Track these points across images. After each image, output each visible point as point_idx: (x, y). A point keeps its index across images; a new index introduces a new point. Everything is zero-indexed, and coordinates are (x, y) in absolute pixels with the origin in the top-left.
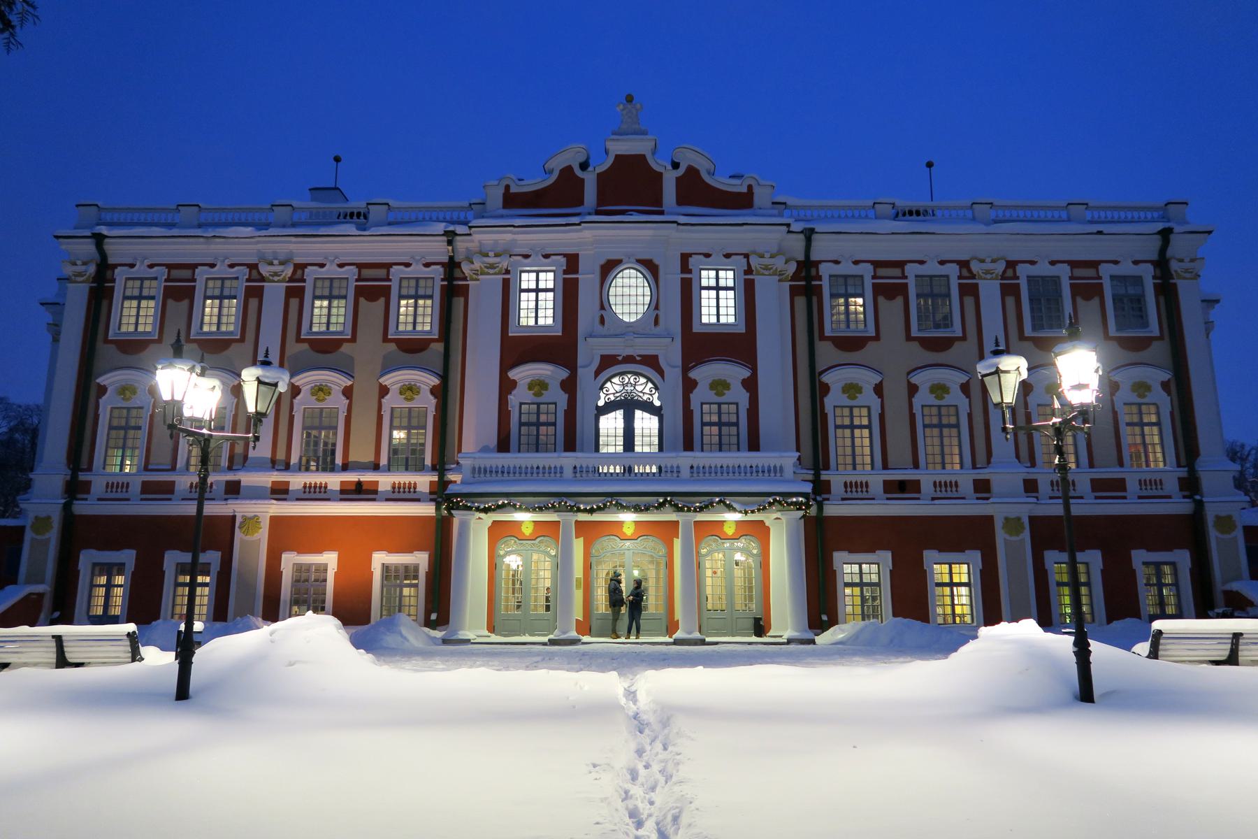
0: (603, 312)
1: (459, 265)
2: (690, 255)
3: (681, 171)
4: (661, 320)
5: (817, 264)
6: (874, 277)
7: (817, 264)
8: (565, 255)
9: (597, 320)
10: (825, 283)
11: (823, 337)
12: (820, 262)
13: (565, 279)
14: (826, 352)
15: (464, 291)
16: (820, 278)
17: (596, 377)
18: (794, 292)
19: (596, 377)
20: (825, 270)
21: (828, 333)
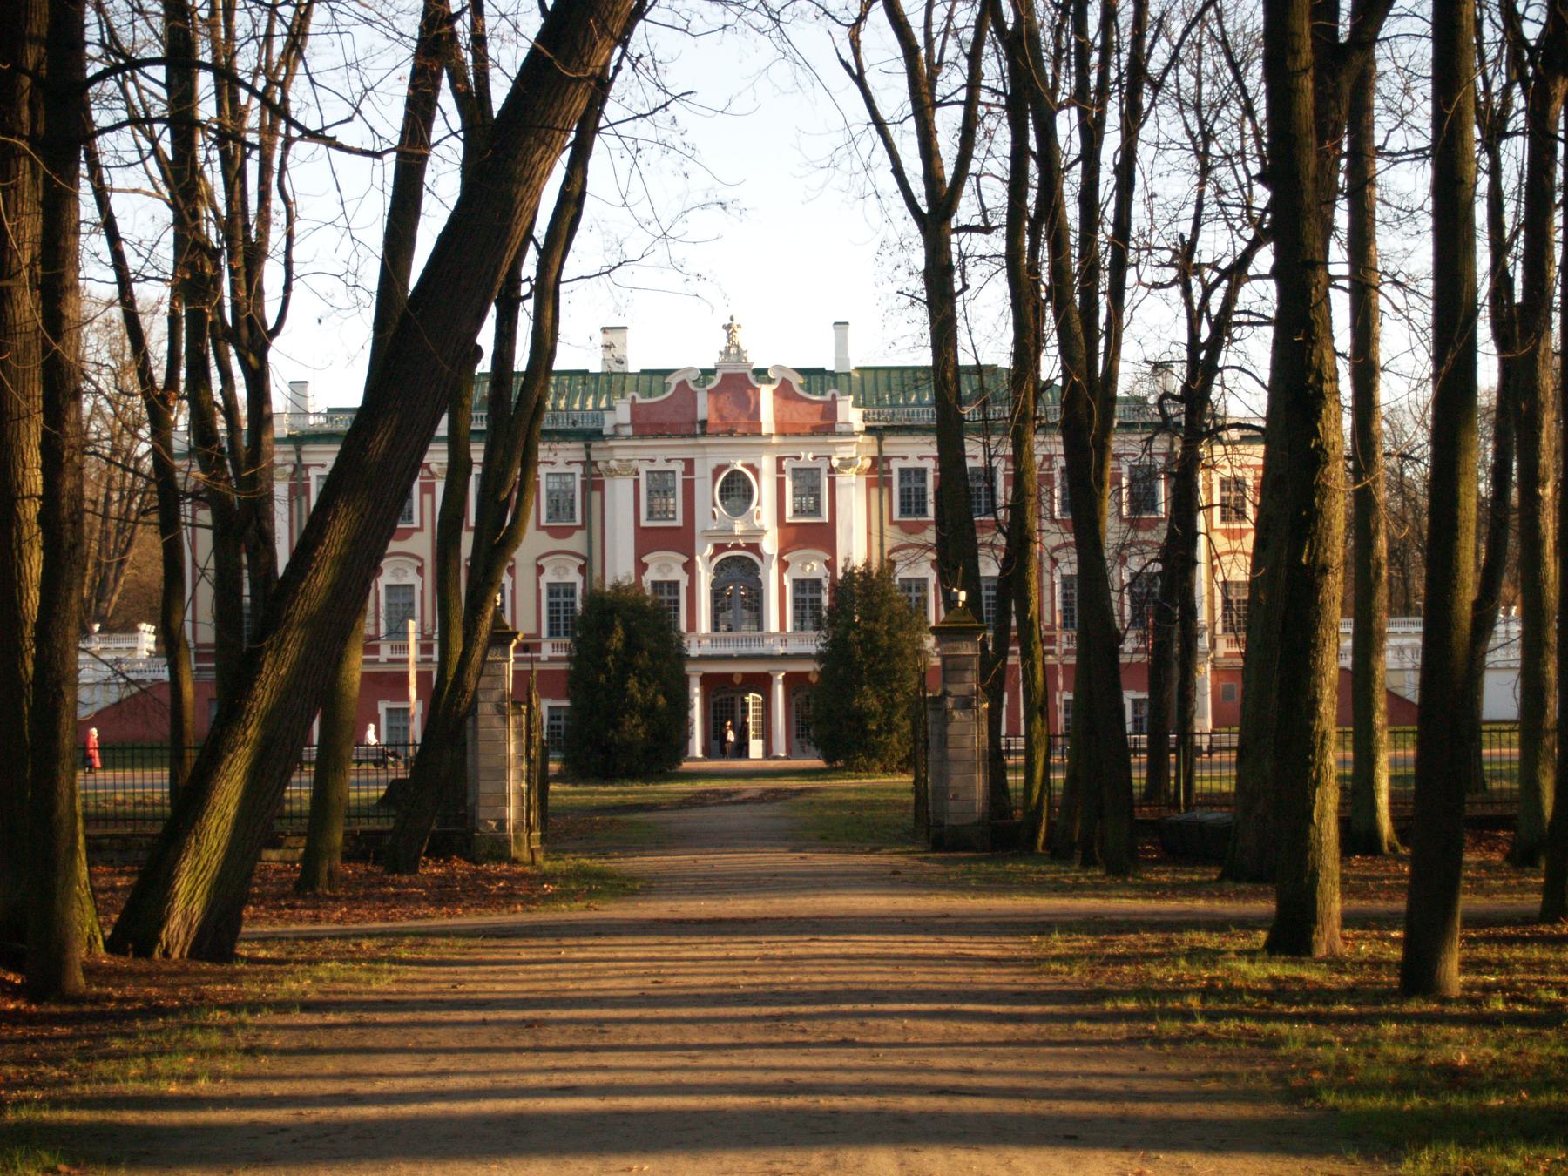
7: (887, 459)
15: (600, 486)
16: (890, 471)
18: (870, 484)
20: (896, 465)
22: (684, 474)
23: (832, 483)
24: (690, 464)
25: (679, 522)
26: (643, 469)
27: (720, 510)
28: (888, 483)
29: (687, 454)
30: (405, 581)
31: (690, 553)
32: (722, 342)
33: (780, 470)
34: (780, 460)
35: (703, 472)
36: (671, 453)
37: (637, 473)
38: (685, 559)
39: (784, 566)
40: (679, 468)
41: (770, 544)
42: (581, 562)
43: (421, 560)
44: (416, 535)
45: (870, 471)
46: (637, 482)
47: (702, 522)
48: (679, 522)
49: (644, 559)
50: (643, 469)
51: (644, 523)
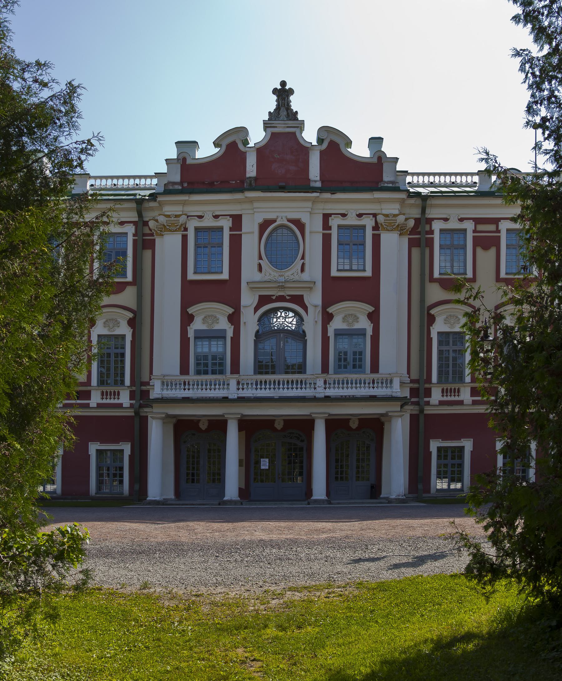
0: (261, 261)
1: (146, 224)
2: (330, 215)
3: (325, 145)
4: (307, 267)
5: (429, 221)
6: (475, 231)
7: (429, 221)
8: (231, 216)
9: (256, 268)
10: (436, 236)
11: (432, 280)
12: (433, 219)
13: (230, 235)
14: (435, 293)
16: (432, 232)
17: (255, 312)
18: (412, 244)
19: (255, 312)
20: (437, 226)
21: (436, 275)
22: (231, 229)
23: (376, 240)
24: (237, 220)
25: (225, 276)
26: (192, 225)
27: (265, 263)
28: (430, 243)
29: (235, 210)
31: (234, 302)
32: (271, 103)
33: (326, 226)
34: (326, 217)
35: (250, 227)
36: (220, 210)
37: (186, 229)
38: (230, 310)
39: (327, 318)
40: (226, 224)
41: (315, 299)
42: (131, 315)
45: (413, 231)
46: (185, 239)
47: (249, 272)
48: (225, 276)
49: (191, 310)
50: (192, 225)
51: (191, 276)
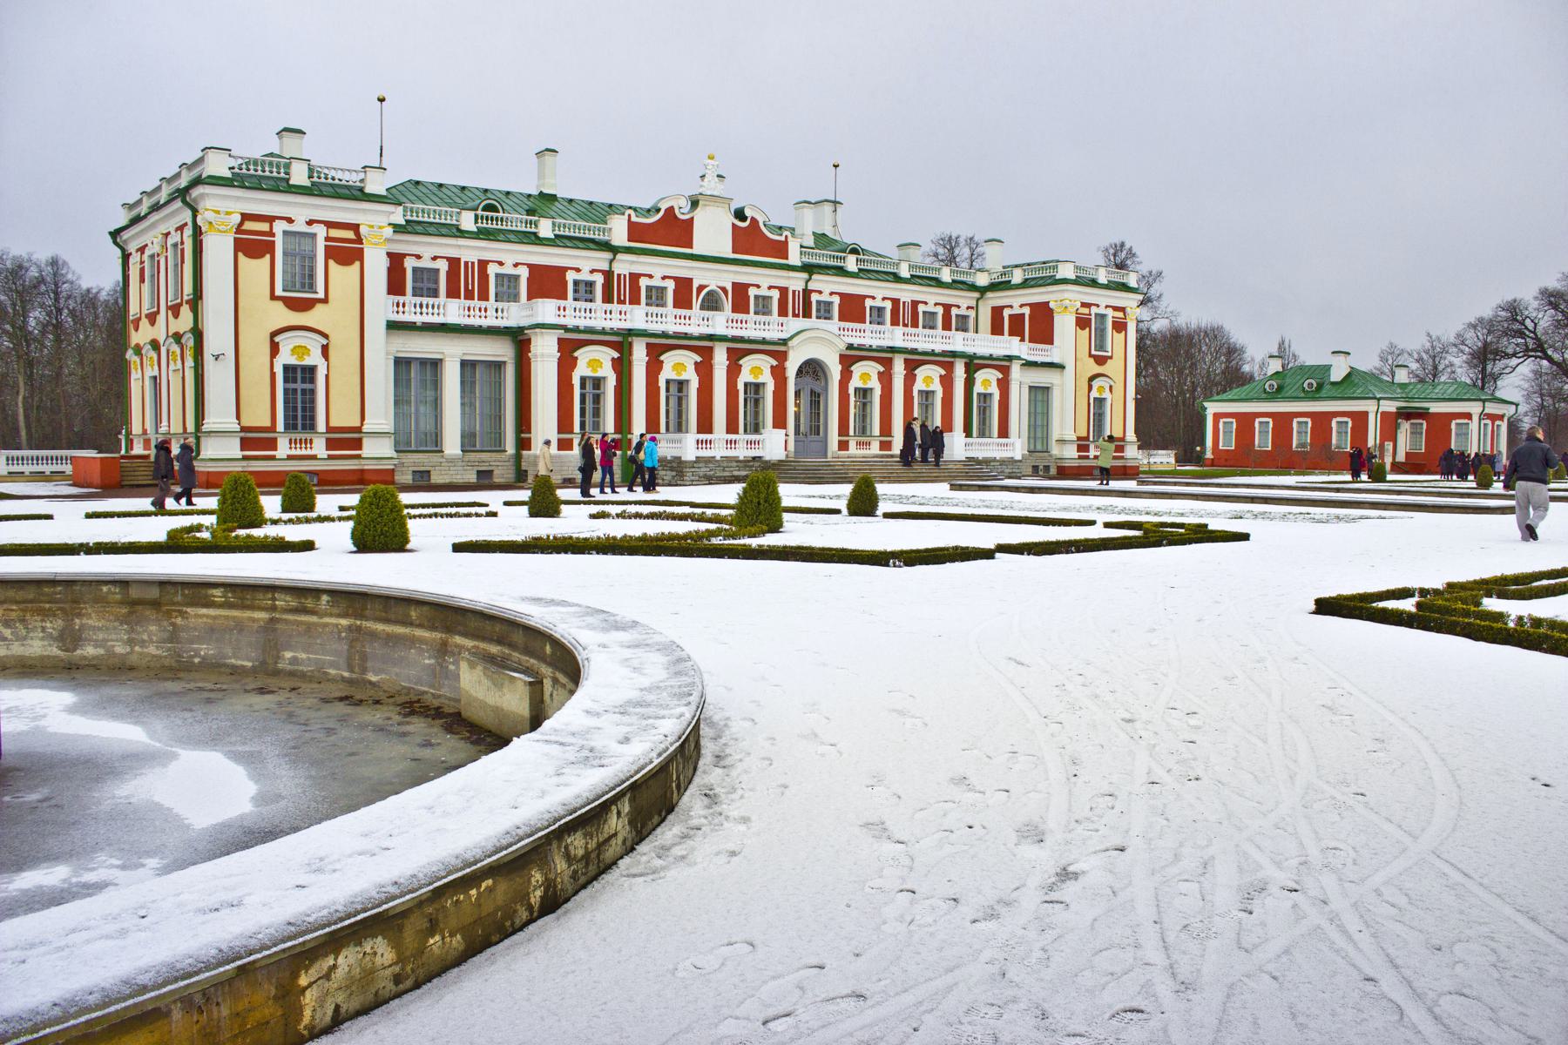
30: (308, 361)
43: (326, 336)
44: (319, 306)
